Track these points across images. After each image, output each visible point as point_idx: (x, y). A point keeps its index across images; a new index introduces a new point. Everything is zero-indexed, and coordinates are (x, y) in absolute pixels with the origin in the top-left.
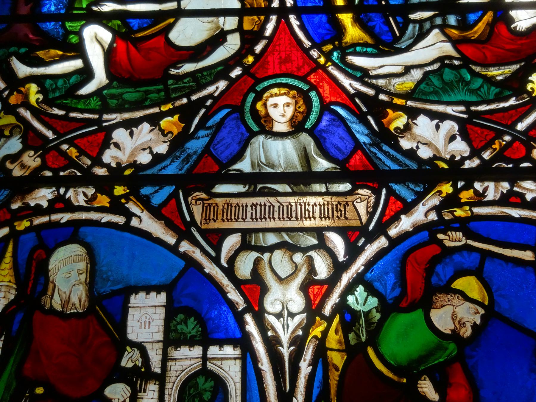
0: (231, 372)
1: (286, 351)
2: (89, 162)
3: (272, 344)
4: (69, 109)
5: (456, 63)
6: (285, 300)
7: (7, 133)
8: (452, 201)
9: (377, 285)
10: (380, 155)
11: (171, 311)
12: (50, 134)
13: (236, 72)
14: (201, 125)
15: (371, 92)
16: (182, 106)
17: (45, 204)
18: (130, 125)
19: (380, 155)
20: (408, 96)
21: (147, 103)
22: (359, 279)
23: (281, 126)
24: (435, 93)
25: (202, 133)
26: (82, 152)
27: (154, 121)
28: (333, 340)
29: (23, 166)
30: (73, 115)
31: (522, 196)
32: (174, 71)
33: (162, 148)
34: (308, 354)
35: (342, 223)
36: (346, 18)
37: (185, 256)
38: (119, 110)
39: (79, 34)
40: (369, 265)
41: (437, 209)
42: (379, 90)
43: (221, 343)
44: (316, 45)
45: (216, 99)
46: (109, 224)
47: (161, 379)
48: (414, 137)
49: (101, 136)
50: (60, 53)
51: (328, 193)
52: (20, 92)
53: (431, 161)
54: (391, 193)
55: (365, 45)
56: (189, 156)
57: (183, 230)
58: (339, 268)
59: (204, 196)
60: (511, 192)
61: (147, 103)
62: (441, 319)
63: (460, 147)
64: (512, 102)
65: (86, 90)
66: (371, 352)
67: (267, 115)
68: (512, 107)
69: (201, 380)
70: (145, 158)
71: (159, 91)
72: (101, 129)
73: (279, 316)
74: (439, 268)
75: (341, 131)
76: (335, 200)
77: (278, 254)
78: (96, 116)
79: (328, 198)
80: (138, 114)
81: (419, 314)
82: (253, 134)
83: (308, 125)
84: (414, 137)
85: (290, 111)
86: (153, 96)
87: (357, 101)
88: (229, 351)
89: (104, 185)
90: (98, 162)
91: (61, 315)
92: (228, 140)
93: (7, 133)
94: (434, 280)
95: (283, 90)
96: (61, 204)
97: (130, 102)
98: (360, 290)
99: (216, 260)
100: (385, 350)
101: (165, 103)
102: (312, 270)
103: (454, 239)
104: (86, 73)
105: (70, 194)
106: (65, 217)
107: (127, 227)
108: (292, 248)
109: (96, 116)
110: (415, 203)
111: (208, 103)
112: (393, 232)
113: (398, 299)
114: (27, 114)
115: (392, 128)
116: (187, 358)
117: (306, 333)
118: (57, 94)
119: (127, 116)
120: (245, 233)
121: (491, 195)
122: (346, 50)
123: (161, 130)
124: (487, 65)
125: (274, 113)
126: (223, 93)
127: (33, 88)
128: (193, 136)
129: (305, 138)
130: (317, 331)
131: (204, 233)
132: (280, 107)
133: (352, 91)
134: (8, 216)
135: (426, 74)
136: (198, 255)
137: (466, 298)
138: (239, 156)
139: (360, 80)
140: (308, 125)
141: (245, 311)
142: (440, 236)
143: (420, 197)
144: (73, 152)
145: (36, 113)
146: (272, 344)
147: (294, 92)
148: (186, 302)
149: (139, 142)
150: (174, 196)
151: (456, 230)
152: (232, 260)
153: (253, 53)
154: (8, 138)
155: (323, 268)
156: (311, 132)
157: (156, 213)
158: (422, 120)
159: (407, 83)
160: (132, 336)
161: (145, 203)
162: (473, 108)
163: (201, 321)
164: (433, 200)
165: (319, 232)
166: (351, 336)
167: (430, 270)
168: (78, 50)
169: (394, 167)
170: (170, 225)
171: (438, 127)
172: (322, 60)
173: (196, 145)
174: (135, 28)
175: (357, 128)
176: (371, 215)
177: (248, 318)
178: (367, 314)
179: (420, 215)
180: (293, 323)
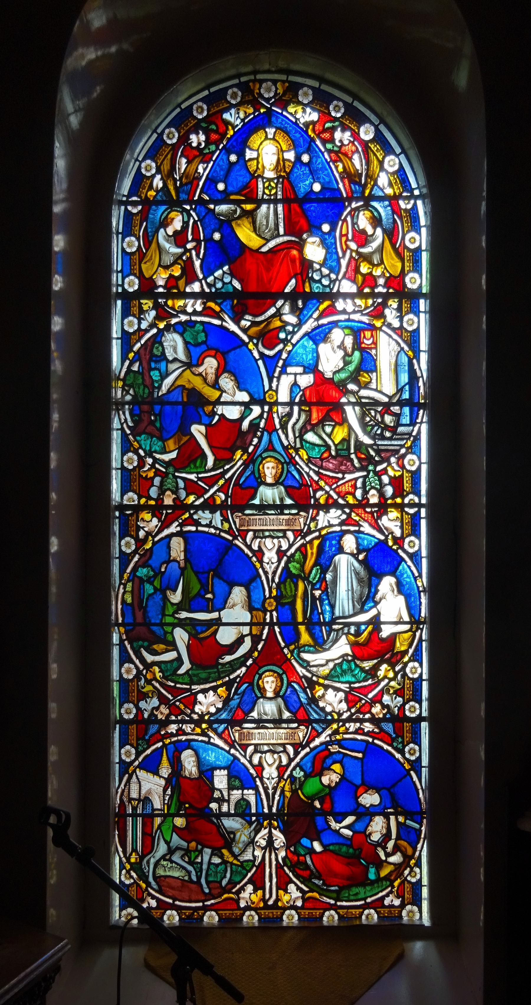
0: (252, 799)
1: (270, 792)
2: (189, 711)
3: (266, 789)
4: (176, 683)
5: (350, 658)
6: (270, 772)
7: (150, 695)
8: (336, 732)
9: (304, 767)
10: (310, 710)
11: (230, 777)
12: (170, 697)
13: (250, 662)
14: (235, 693)
15: (309, 675)
16: (226, 682)
17: (175, 732)
18: (204, 691)
19: (310, 710)
20: (325, 678)
21: (211, 680)
22: (298, 765)
23: (270, 694)
24: (338, 676)
25: (236, 697)
26: (186, 707)
27: (215, 689)
28: (287, 788)
29: (162, 713)
30: (178, 686)
31: (363, 729)
32: (221, 661)
33: (220, 705)
34: (278, 793)
35: (292, 742)
36: (302, 628)
37: (233, 755)
38: (199, 684)
39: (172, 633)
40: (302, 759)
41: (330, 735)
42: (313, 675)
43: (248, 789)
44: (287, 646)
45: (241, 678)
46: (202, 741)
47: (228, 801)
48: (325, 701)
49: (192, 697)
50: (165, 647)
51: (288, 728)
52: (151, 671)
53: (330, 714)
54: (313, 728)
55: (310, 646)
56: (231, 709)
57: (232, 745)
58: (291, 760)
59: (238, 728)
60: (360, 728)
61: (211, 680)
62: (325, 780)
63: (344, 706)
64: (370, 682)
65: (182, 671)
66: (299, 791)
67: (264, 687)
68: (370, 685)
69: (242, 802)
70: (213, 710)
71: (215, 673)
72: (192, 694)
73: (268, 779)
74: (327, 760)
75: (295, 697)
76: (290, 731)
77: (268, 754)
78: (188, 687)
79: (288, 730)
80: (207, 686)
81: (318, 778)
82: (258, 698)
83: (281, 693)
84: (325, 701)
85: (274, 686)
86: (212, 675)
87: (303, 680)
88: (251, 791)
89: (198, 723)
90: (193, 712)
91: (189, 778)
92: (248, 701)
93: (150, 695)
94: (325, 765)
95: (271, 673)
96: (180, 732)
97: (202, 679)
98: (298, 768)
99: (245, 757)
100: (304, 791)
101: (219, 680)
102: (281, 761)
103: (334, 748)
104: (179, 660)
105: (184, 727)
106: (184, 738)
107: (209, 743)
108: (273, 752)
109: (188, 687)
110: (322, 732)
111: (238, 680)
112: (312, 745)
113: (311, 773)
114: (157, 685)
115: (317, 696)
116: (236, 794)
117: (278, 784)
118: (169, 674)
119: (202, 687)
120: (256, 745)
121: (351, 730)
122: (301, 649)
123: (218, 695)
124: (363, 660)
125: (267, 687)
126: (244, 674)
127: (156, 669)
128: (232, 699)
129: (280, 700)
130: (281, 785)
131: (240, 745)
132: (269, 683)
133: (301, 675)
134: (160, 737)
135: (335, 665)
136: (238, 754)
137: (335, 772)
138: (252, 710)
139: (305, 668)
140: (281, 693)
141: (256, 777)
142: (329, 747)
143: (324, 730)
144: (182, 707)
145: (161, 684)
146: (266, 789)
147: (276, 675)
148: (235, 773)
149: (210, 701)
150: (226, 728)
151: (336, 744)
152: (251, 757)
153: (257, 651)
154: (152, 698)
155: (285, 761)
156: (283, 697)
157: (220, 736)
158: (330, 691)
159: (325, 671)
160: (216, 786)
161: (215, 731)
162: (352, 685)
163: (241, 781)
164: (328, 732)
165: (283, 745)
166: (293, 786)
167: (324, 761)
168: (173, 645)
169: (316, 716)
170: (226, 742)
171: (336, 695)
172: (289, 656)
173: (234, 703)
174: (199, 631)
175: (302, 695)
176: (304, 738)
177: (257, 779)
178: (299, 778)
179: (323, 738)
180: (273, 781)
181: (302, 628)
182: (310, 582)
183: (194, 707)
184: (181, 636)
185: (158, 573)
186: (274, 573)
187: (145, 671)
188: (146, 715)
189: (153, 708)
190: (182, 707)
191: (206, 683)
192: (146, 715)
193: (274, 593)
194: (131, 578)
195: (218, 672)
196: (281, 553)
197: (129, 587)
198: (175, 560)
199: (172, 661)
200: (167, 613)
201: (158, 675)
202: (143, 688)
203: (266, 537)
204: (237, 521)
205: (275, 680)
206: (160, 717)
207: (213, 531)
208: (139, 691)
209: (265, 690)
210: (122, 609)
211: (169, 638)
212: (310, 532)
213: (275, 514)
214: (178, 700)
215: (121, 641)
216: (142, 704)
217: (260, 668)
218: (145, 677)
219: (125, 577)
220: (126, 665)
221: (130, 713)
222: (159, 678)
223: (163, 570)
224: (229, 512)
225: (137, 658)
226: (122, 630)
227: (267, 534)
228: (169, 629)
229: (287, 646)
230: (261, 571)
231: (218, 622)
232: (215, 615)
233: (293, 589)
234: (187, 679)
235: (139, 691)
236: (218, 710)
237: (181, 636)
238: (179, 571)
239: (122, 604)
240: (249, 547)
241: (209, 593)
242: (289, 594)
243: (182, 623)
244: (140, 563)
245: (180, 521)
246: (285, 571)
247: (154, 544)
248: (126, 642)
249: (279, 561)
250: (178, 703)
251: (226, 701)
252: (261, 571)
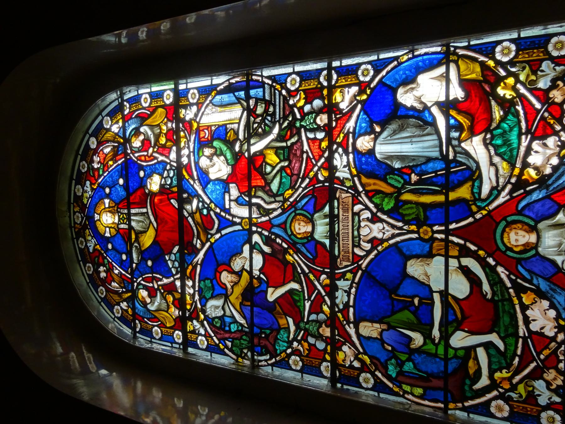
2: (553, 344)
4: (515, 354)
7: (531, 389)
13: (491, 261)
14: (530, 282)
16: (515, 292)
21: (512, 311)
23: (533, 238)
25: (535, 281)
26: (547, 347)
27: (524, 308)
29: (555, 379)
30: (519, 352)
32: (489, 296)
36: (453, 196)
39: (456, 349)
49: (534, 336)
50: (471, 361)
52: (501, 383)
55: (473, 187)
67: (523, 245)
70: (552, 313)
71: (503, 305)
72: (530, 337)
78: (521, 340)
82: (537, 253)
83: (532, 223)
85: (521, 233)
93: (531, 389)
95: (505, 235)
104: (488, 346)
109: (521, 340)
111: (514, 278)
114: (517, 378)
118: (503, 361)
122: (476, 198)
125: (522, 241)
126: (506, 269)
127: (497, 375)
128: (538, 287)
129: (541, 226)
132: (518, 238)
140: (532, 223)
144: (546, 352)
147: (507, 230)
153: (477, 251)
154: (534, 388)
156: (537, 222)
168: (470, 351)
172: (484, 212)
174: (454, 317)
181: (453, 196)
182: (403, 187)
183: (547, 337)
184: (460, 340)
185: (393, 354)
186: (393, 226)
187: (500, 390)
188: (558, 400)
189: (548, 388)
190: (546, 352)
191: (517, 318)
192: (558, 400)
193: (414, 227)
194: (398, 384)
195: (503, 300)
196: (374, 219)
197: (407, 388)
198: (381, 334)
199: (489, 356)
200: (434, 351)
201: (505, 374)
202: (521, 396)
203: (359, 235)
204: (345, 263)
205: (514, 231)
206: (559, 382)
207: (353, 290)
208: (524, 402)
209: (527, 244)
210: (430, 401)
211: (461, 353)
212: (354, 187)
213: (338, 223)
214: (538, 356)
215: (464, 409)
216: (543, 401)
217: (498, 248)
218: (507, 391)
219: (396, 389)
220: (493, 410)
221: (553, 418)
222: (509, 375)
223: (390, 348)
224: (336, 271)
225: (483, 395)
226: (451, 406)
227: (356, 233)
228: (451, 352)
229: (472, 214)
230: (391, 242)
231: (444, 294)
232: (437, 298)
233: (409, 205)
234: (511, 340)
235: (524, 402)
236: (552, 306)
237: (460, 340)
238: (391, 331)
239: (424, 399)
240: (369, 253)
241: (413, 302)
242: (414, 210)
243: (446, 337)
244: (383, 371)
245: (345, 322)
246: (391, 215)
247: (365, 353)
248: (466, 404)
249: (382, 221)
250: (542, 357)
251: (541, 295)
252: (391, 242)
